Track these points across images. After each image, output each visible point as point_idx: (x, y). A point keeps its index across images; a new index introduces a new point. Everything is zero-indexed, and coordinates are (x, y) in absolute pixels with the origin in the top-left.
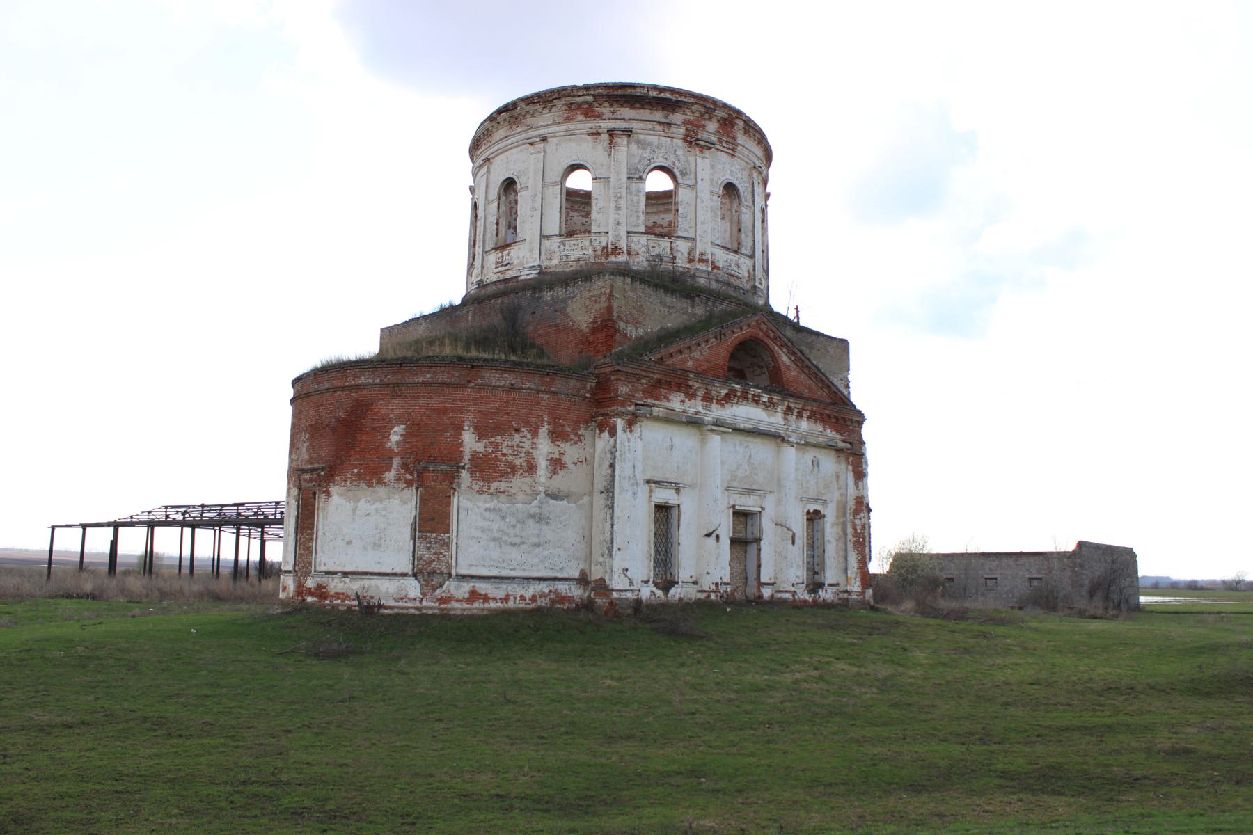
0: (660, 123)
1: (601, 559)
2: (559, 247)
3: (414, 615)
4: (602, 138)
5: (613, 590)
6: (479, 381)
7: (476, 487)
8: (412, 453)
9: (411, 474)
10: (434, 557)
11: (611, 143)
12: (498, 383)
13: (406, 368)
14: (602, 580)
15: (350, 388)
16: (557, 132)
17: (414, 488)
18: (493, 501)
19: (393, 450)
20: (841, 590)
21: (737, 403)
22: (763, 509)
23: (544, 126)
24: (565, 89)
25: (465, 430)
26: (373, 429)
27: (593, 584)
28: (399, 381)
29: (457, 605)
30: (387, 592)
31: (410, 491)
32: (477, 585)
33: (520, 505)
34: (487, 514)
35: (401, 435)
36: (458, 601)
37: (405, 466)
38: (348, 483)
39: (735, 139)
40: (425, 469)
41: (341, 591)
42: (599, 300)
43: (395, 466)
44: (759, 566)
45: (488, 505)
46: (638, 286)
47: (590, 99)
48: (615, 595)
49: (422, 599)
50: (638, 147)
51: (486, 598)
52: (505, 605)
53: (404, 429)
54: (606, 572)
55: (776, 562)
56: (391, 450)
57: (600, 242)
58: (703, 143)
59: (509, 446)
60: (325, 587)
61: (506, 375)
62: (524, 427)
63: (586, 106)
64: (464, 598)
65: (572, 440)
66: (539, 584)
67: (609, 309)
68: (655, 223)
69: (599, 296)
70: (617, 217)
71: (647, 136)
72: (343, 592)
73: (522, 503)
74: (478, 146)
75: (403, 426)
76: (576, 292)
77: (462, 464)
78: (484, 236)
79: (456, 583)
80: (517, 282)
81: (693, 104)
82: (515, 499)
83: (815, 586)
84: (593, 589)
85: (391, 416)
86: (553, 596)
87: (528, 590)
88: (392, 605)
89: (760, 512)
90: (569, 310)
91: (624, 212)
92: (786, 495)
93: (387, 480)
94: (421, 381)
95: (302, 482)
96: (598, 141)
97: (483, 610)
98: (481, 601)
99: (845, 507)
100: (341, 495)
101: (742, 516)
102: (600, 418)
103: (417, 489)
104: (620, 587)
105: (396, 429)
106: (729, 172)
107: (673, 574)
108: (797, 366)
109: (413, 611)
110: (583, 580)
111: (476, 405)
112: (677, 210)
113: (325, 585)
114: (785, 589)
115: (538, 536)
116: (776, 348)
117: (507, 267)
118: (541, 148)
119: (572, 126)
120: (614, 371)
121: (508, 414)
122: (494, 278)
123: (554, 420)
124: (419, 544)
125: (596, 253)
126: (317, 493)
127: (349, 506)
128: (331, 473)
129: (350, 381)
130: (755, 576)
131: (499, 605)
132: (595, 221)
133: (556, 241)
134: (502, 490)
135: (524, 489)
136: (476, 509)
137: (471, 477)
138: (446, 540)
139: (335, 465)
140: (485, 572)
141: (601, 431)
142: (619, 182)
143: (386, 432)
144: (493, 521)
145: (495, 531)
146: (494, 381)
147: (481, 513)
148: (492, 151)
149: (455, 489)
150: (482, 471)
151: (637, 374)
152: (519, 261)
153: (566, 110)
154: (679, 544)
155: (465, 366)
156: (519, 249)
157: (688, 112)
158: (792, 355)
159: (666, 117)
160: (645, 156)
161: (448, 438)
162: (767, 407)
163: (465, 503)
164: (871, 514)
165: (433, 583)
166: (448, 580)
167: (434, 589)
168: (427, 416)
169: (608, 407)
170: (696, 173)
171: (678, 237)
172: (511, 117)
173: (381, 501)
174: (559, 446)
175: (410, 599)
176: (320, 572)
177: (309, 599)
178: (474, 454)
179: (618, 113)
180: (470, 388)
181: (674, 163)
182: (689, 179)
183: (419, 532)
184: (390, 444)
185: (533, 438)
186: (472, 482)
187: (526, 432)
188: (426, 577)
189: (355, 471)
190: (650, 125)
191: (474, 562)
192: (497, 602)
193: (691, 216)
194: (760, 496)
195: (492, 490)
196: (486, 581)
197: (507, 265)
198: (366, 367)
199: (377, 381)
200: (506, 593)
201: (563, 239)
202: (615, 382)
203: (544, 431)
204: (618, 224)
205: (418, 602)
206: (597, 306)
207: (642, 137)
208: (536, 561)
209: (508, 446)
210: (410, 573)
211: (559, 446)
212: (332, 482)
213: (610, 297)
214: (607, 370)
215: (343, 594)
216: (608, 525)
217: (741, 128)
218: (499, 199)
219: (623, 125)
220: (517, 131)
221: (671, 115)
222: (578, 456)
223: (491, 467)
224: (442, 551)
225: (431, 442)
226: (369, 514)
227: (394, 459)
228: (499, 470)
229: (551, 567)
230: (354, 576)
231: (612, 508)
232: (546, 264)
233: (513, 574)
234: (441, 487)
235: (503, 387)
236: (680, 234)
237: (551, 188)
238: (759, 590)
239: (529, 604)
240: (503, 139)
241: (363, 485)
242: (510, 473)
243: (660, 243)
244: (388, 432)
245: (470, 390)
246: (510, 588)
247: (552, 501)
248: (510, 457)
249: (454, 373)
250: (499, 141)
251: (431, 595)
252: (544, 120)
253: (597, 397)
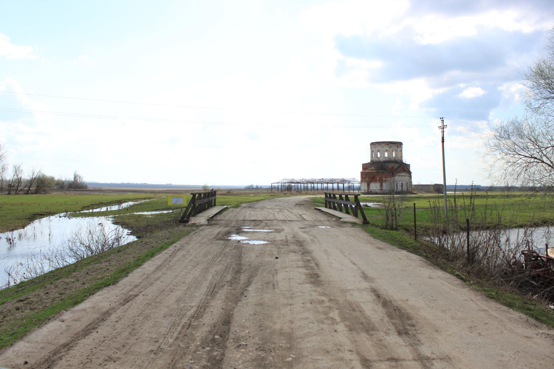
83: (407, 190)
101: (402, 184)
252: (383, 144)
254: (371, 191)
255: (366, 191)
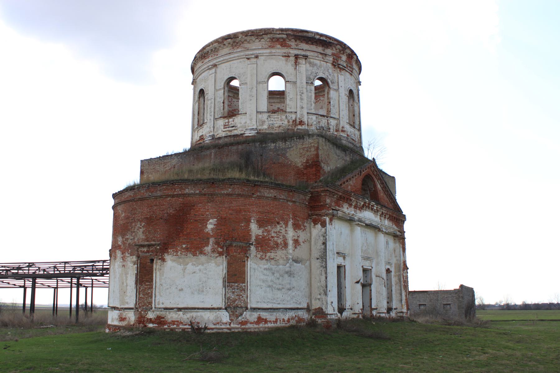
0: (321, 53)
1: (319, 297)
2: (267, 119)
3: (227, 333)
4: (291, 59)
5: (328, 314)
6: (259, 194)
7: (259, 256)
8: (221, 235)
9: (222, 248)
10: (237, 297)
11: (296, 62)
12: (268, 196)
13: (216, 185)
14: (320, 309)
15: (178, 196)
16: (264, 53)
17: (224, 257)
18: (268, 264)
19: (209, 234)
20: (398, 311)
21: (365, 210)
22: (372, 268)
23: (256, 49)
24: (269, 29)
25: (251, 222)
26: (196, 221)
27: (313, 311)
28: (212, 193)
29: (251, 326)
30: (209, 319)
31: (221, 258)
32: (261, 313)
33: (281, 266)
34: (265, 272)
35: (214, 225)
36: (251, 323)
37: (217, 243)
38: (179, 253)
39: (352, 65)
40: (231, 245)
41: (176, 320)
42: (310, 150)
43: (211, 243)
44: (371, 299)
45: (265, 267)
46: (328, 144)
47: (284, 36)
48: (329, 317)
49: (230, 323)
50: (310, 66)
51: (266, 321)
52: (275, 324)
53: (216, 221)
54: (323, 304)
55: (377, 297)
56: (208, 233)
57: (292, 117)
58: (341, 67)
59: (274, 231)
60: (163, 318)
61: (272, 191)
62: (281, 221)
63: (282, 40)
64: (254, 321)
65: (302, 229)
66: (291, 312)
67: (317, 155)
68: (279, 108)
69: (310, 148)
70: (301, 104)
71: (314, 61)
72: (178, 320)
73: (282, 265)
74: (204, 57)
75: (216, 220)
76: (293, 145)
77: (251, 242)
78: (214, 109)
79: (250, 313)
80: (243, 137)
81: (337, 45)
82: (279, 263)
83: (389, 310)
84: (314, 314)
85: (208, 213)
86: (297, 319)
87: (286, 315)
88: (211, 327)
89: (371, 269)
90: (288, 155)
91: (305, 101)
92: (381, 260)
93: (206, 252)
94: (225, 192)
95: (139, 252)
96: (288, 60)
97: (266, 328)
98: (263, 323)
99: (400, 268)
100: (174, 261)
101: (365, 271)
102: (314, 217)
103: (226, 257)
104: (331, 313)
105: (211, 221)
106: (350, 83)
107: (343, 304)
108: (383, 190)
109: (226, 330)
110: (308, 309)
111: (257, 208)
112: (330, 103)
113: (163, 316)
114: (383, 312)
115: (290, 284)
116: (376, 180)
117: (233, 128)
118: (255, 62)
119: (273, 51)
120: (324, 190)
121: (273, 213)
122: (224, 134)
123: (294, 218)
124: (228, 290)
125: (289, 123)
126: (155, 260)
127: (180, 268)
128: (166, 247)
129: (178, 192)
130: (369, 305)
131: (273, 325)
132: (288, 105)
133: (265, 115)
134: (272, 257)
135: (282, 257)
136: (259, 268)
137: (256, 250)
138: (244, 287)
139: (168, 243)
140: (265, 306)
141: (315, 224)
142: (302, 85)
143: (205, 223)
144: (268, 276)
145: (269, 282)
146: (266, 194)
147: (262, 272)
148: (218, 60)
149: (248, 257)
150: (262, 247)
151: (334, 193)
152: (241, 125)
153: (270, 41)
154: (345, 287)
155: (251, 185)
156: (241, 118)
157: (334, 49)
158: (382, 184)
159: (324, 50)
160: (314, 71)
161: (243, 227)
162: (375, 212)
163: (254, 266)
164: (408, 271)
165: (237, 313)
166: (245, 311)
167: (237, 317)
168: (230, 214)
169: (320, 210)
170: (338, 82)
171: (331, 117)
172: (234, 42)
173: (203, 265)
174: (297, 232)
175: (223, 323)
176: (160, 308)
177: (151, 325)
178: (257, 236)
179: (299, 46)
180: (254, 198)
181: (328, 76)
182: (335, 86)
183: (227, 283)
184: (207, 230)
185: (286, 228)
186: (256, 253)
187: (282, 224)
188: (233, 310)
189: (184, 246)
190: (316, 54)
191: (259, 300)
192: (271, 323)
193: (337, 106)
194: (370, 261)
195: (267, 258)
196: (266, 311)
197: (232, 127)
198: (189, 183)
199: (198, 192)
200: (276, 318)
201: (270, 114)
202: (324, 197)
203: (290, 223)
204: (302, 108)
205: (228, 325)
206: (309, 153)
207: (312, 60)
208: (289, 298)
209: (274, 232)
210: (224, 307)
211: (297, 232)
212: (166, 253)
213: (317, 149)
214: (319, 190)
215: (178, 321)
216: (323, 278)
217: (355, 60)
218: (224, 88)
219: (303, 53)
220: (238, 51)
221: (326, 50)
222: (304, 238)
223: (266, 244)
224: (241, 294)
225: (233, 229)
226: (195, 272)
227: (210, 239)
228: (270, 246)
229: (296, 302)
230: (186, 310)
231: (326, 267)
232: (260, 128)
233: (279, 306)
234: (240, 256)
235: (271, 197)
236: (332, 116)
237: (261, 85)
238: (371, 313)
239: (286, 324)
240: (227, 54)
241: (190, 255)
242: (276, 248)
243: (323, 120)
244: (205, 223)
245: (253, 199)
246: (278, 315)
247: (295, 264)
248: (276, 239)
249: (244, 188)
250: (224, 55)
251: (236, 320)
252: (256, 46)
253: (311, 205)
254: (160, 320)
255: (132, 317)
